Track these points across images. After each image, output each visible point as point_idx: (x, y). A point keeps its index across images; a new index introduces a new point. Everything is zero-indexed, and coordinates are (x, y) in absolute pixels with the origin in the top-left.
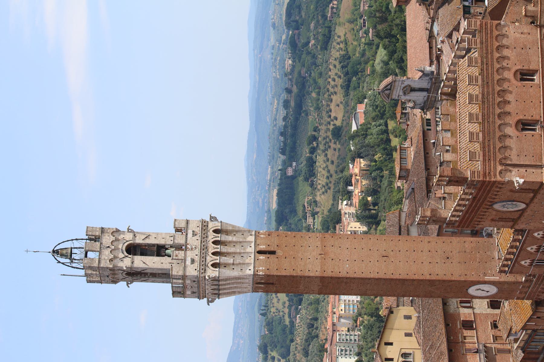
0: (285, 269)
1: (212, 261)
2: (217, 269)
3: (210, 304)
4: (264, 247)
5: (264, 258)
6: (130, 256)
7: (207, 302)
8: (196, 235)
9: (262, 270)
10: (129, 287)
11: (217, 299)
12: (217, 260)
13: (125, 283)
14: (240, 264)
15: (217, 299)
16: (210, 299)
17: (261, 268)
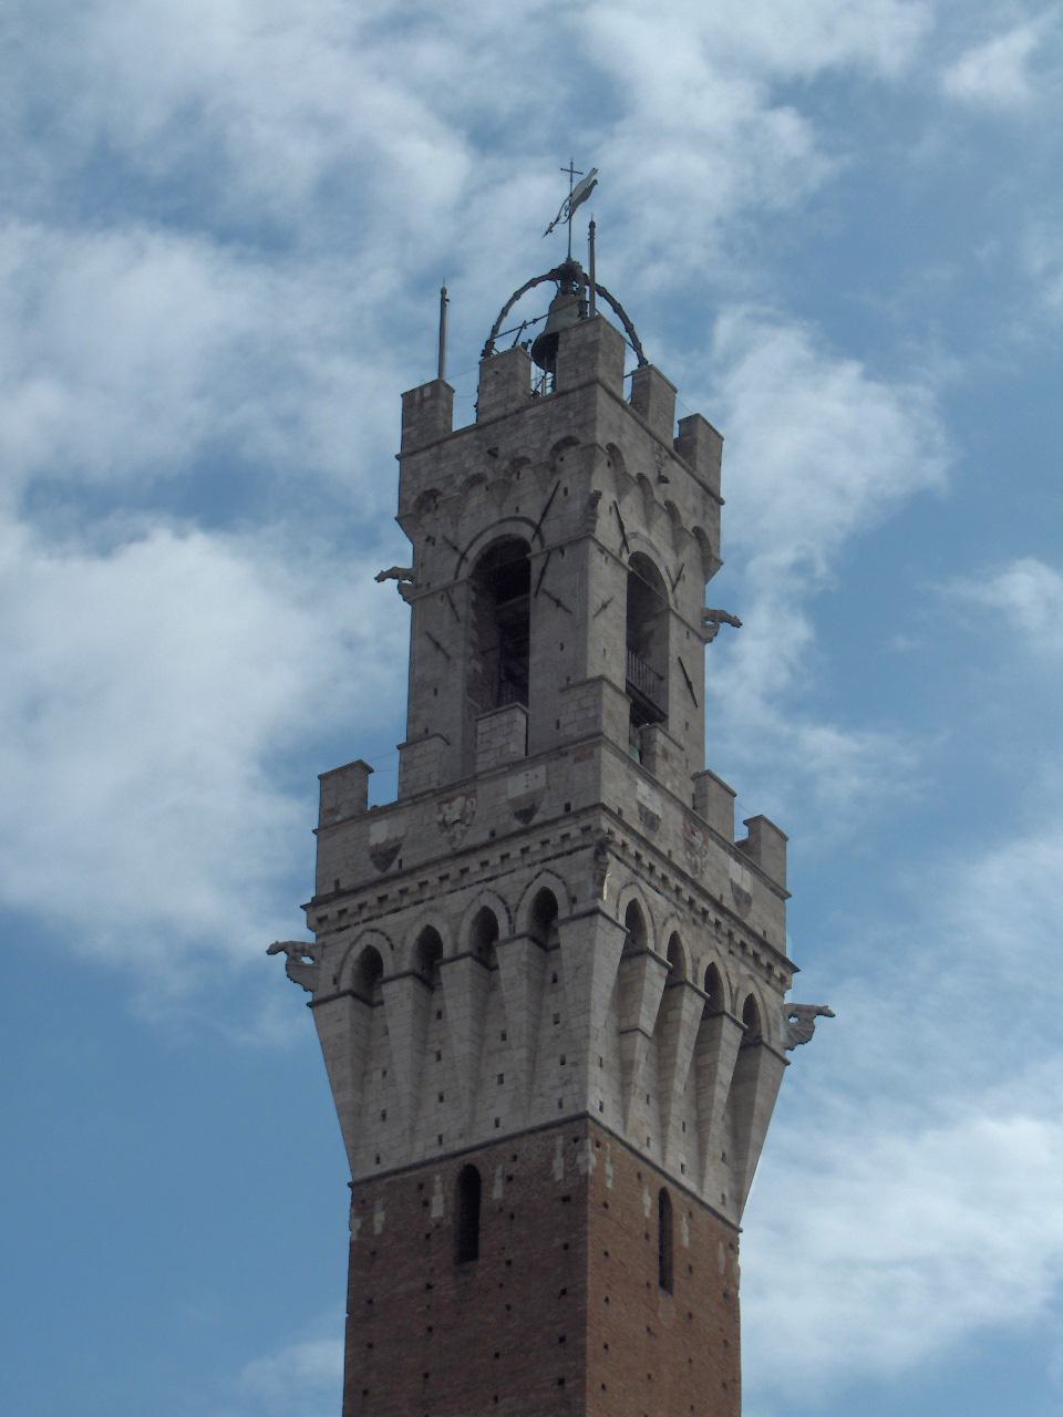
0: (607, 1300)
1: (651, 913)
2: (622, 921)
3: (282, 956)
4: (686, 1241)
5: (647, 1214)
6: (625, 558)
7: (293, 944)
8: (737, 902)
9: (600, 1169)
10: (380, 578)
11: (309, 997)
12: (657, 942)
13: (406, 563)
14: (626, 1067)
15: (309, 997)
16: (307, 960)
17: (609, 1170)
